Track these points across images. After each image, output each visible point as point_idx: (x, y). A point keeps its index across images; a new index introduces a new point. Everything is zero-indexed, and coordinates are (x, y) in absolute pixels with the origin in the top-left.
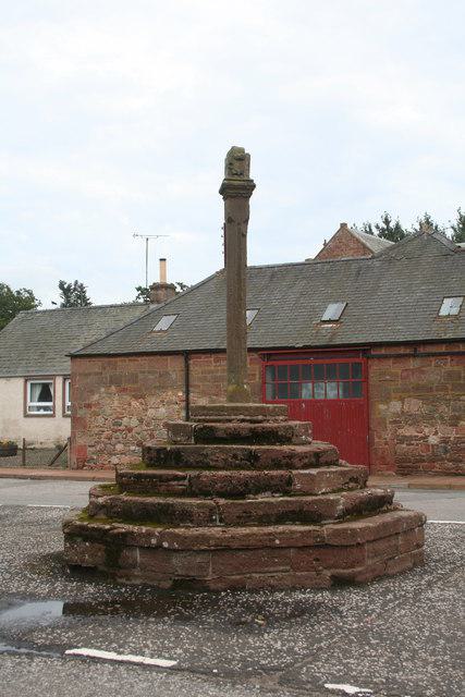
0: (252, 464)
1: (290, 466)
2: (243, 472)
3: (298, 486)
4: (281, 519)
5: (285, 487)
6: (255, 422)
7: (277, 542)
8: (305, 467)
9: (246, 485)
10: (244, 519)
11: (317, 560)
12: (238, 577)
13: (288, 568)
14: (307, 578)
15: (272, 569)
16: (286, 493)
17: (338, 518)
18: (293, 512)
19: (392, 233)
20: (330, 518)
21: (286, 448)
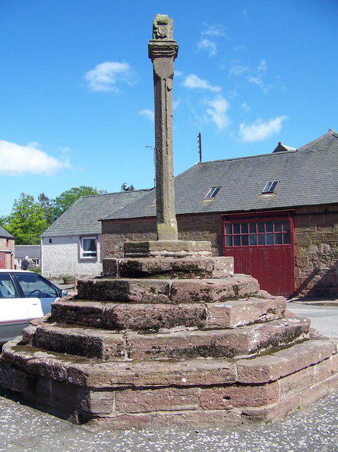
0: (170, 298)
1: (208, 299)
2: (157, 306)
3: (213, 320)
4: (192, 353)
5: (198, 321)
6: (179, 257)
7: (184, 380)
8: (223, 299)
9: (160, 319)
10: (154, 353)
11: (227, 398)
12: (144, 414)
13: (196, 406)
14: (216, 416)
15: (179, 407)
16: (201, 327)
17: (252, 352)
18: (205, 347)
19: (76, 190)
20: (243, 353)
21: (204, 282)
